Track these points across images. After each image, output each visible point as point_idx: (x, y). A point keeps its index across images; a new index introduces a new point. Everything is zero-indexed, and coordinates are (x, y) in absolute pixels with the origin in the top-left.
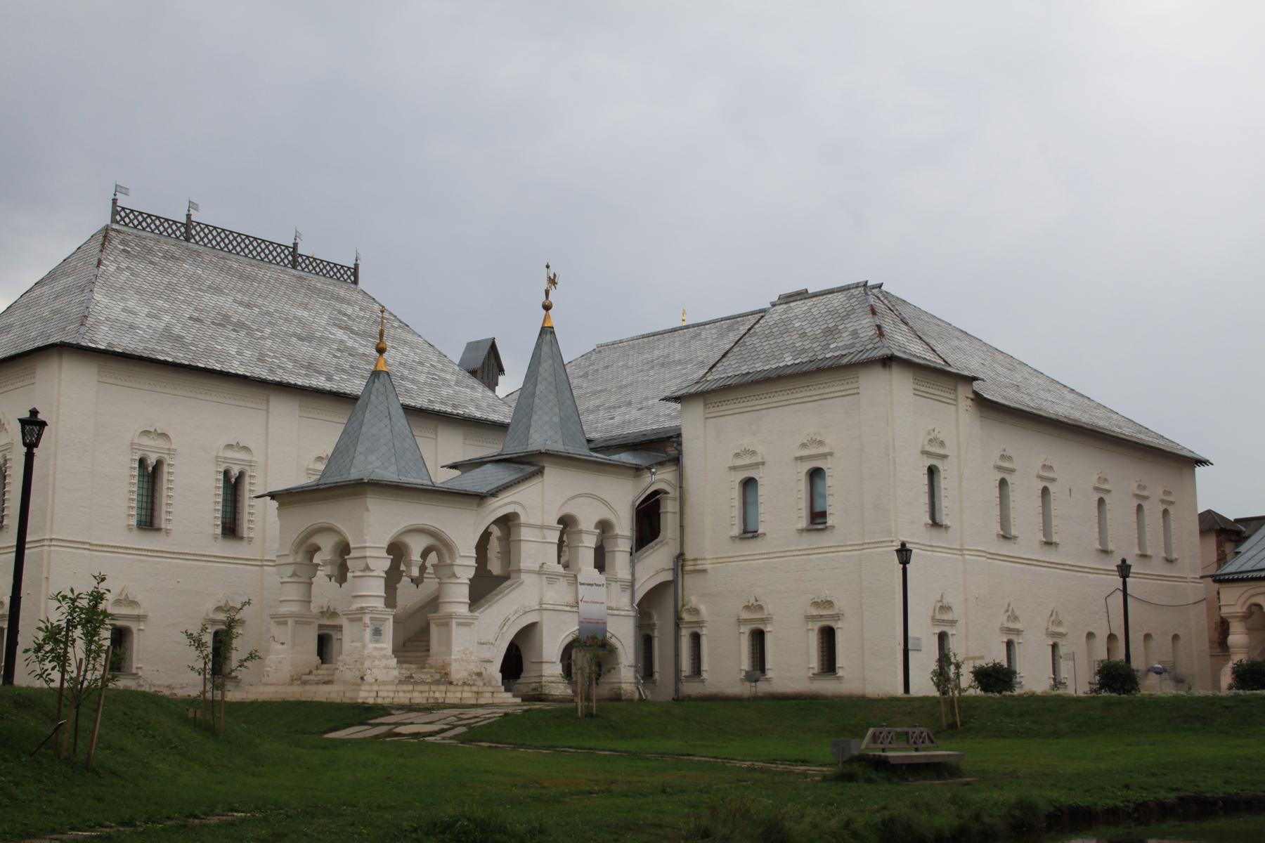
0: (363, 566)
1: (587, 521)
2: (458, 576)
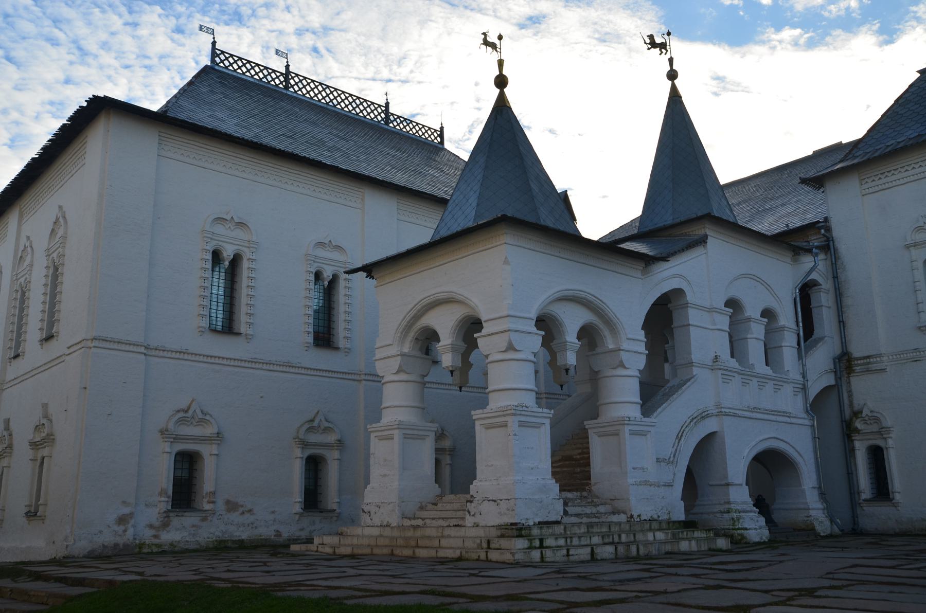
0: (504, 345)
1: (752, 310)
2: (627, 366)
